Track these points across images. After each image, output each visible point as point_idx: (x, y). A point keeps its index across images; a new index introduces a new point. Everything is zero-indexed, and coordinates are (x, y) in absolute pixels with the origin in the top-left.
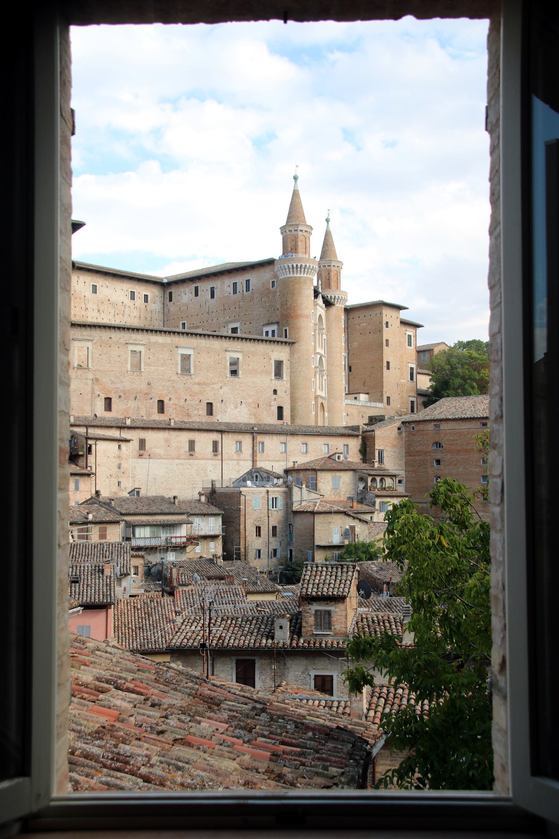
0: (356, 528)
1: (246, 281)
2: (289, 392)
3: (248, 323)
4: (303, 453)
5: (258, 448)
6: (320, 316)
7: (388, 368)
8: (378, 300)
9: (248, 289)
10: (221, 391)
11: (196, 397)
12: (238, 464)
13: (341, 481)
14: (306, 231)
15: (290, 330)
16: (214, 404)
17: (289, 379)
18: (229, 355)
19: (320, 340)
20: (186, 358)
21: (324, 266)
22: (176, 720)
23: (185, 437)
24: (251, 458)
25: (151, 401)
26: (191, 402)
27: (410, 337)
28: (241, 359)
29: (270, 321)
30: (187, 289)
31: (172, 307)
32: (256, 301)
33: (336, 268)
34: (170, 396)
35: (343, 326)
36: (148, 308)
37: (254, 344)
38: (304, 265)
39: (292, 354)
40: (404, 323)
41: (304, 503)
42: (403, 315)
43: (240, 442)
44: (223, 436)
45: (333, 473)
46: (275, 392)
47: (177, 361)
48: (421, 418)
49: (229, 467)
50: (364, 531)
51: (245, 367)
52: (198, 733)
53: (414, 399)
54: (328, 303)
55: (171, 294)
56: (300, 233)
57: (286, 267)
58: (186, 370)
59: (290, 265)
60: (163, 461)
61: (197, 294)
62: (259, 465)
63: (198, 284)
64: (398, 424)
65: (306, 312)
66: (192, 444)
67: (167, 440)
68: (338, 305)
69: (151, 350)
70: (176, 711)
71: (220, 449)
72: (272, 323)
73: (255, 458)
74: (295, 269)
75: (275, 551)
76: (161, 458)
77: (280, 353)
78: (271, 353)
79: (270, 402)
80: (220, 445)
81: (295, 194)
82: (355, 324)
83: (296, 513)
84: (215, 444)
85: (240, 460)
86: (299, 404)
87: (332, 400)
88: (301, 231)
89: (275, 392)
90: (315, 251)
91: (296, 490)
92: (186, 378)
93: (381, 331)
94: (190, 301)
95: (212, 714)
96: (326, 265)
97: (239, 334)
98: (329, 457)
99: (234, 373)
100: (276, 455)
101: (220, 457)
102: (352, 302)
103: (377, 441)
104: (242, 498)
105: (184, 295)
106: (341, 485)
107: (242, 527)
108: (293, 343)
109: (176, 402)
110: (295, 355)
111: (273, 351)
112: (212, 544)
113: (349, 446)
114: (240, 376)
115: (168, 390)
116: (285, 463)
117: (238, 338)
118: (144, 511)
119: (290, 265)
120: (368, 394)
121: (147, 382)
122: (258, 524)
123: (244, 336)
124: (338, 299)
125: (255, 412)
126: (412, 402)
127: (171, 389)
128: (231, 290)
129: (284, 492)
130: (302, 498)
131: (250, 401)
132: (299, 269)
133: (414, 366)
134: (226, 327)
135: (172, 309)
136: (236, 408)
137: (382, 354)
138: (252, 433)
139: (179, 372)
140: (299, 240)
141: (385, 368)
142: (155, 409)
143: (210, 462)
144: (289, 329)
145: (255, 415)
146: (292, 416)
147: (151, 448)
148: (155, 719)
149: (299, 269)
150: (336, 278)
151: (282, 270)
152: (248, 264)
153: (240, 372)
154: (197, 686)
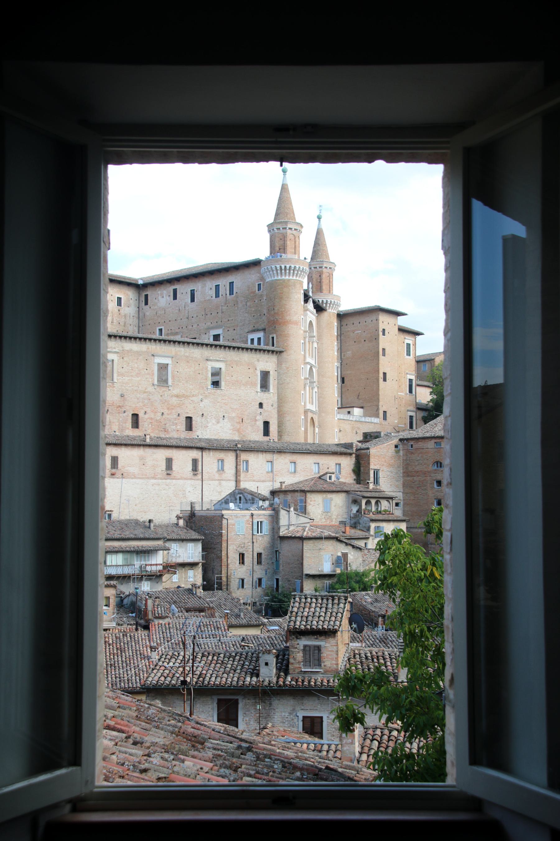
0: (349, 555)
1: (230, 283)
2: (276, 405)
3: (231, 330)
4: (291, 473)
5: (242, 467)
6: (311, 322)
7: (385, 380)
8: (374, 305)
9: (231, 293)
10: (202, 404)
11: (174, 411)
12: (220, 484)
13: (333, 503)
14: (295, 229)
15: (277, 338)
16: (193, 419)
17: (276, 391)
18: (211, 365)
19: (312, 349)
20: (163, 368)
22: (159, 759)
23: (161, 455)
24: (233, 478)
25: (125, 415)
26: (168, 417)
27: (408, 345)
28: (223, 370)
29: (256, 327)
30: (165, 292)
31: (148, 311)
32: (240, 305)
34: (146, 409)
35: (336, 334)
36: (122, 311)
37: (237, 353)
38: (293, 266)
39: (279, 364)
40: (402, 330)
41: (292, 528)
42: (402, 321)
43: (222, 461)
44: (204, 453)
45: (324, 495)
46: (261, 405)
47: (153, 371)
48: (421, 435)
49: (210, 487)
50: (357, 559)
51: (228, 378)
52: (182, 772)
54: (319, 309)
55: (146, 296)
56: (289, 231)
57: (274, 269)
58: (163, 381)
59: (278, 266)
60: (138, 481)
61: (175, 298)
62: (243, 485)
63: (177, 286)
64: (395, 441)
65: (295, 318)
66: (169, 462)
67: (142, 458)
68: (330, 310)
69: (125, 359)
70: (159, 749)
71: (200, 468)
72: (258, 330)
73: (239, 478)
74: (283, 271)
76: (135, 478)
77: (267, 363)
78: (256, 363)
79: (256, 417)
80: (200, 463)
81: (284, 189)
82: (348, 331)
83: (283, 538)
84: (195, 462)
85: (222, 480)
86: (288, 418)
87: (323, 414)
88: (290, 229)
89: (261, 405)
90: (306, 250)
91: (283, 513)
92: (164, 389)
93: (377, 339)
94: (168, 305)
95: (196, 753)
96: (318, 266)
97: (221, 342)
98: (320, 478)
99: (216, 384)
100: (263, 475)
101: (200, 477)
102: (346, 306)
103: (372, 460)
104: (224, 522)
105: (161, 298)
106: (333, 508)
107: (224, 553)
108: (281, 352)
109: (152, 416)
110: (283, 365)
111: (258, 361)
112: (191, 573)
113: (342, 465)
114: (222, 388)
115: (143, 403)
116: (271, 483)
117: (221, 346)
118: (117, 536)
119: (278, 266)
120: (362, 408)
121: (120, 393)
122: (241, 551)
124: (330, 304)
125: (238, 427)
126: (411, 417)
127: (146, 401)
128: (213, 293)
132: (288, 271)
133: (413, 377)
134: (208, 334)
135: (147, 314)
136: (218, 422)
137: (378, 364)
138: (236, 450)
139: (156, 382)
140: (288, 239)
141: (381, 380)
142: (129, 424)
143: (189, 482)
144: (277, 336)
145: (238, 430)
146: (279, 432)
147: (123, 467)
148: (137, 757)
149: (288, 271)
150: (328, 281)
151: (269, 272)
152: (232, 265)
153: (223, 384)
154: (180, 724)
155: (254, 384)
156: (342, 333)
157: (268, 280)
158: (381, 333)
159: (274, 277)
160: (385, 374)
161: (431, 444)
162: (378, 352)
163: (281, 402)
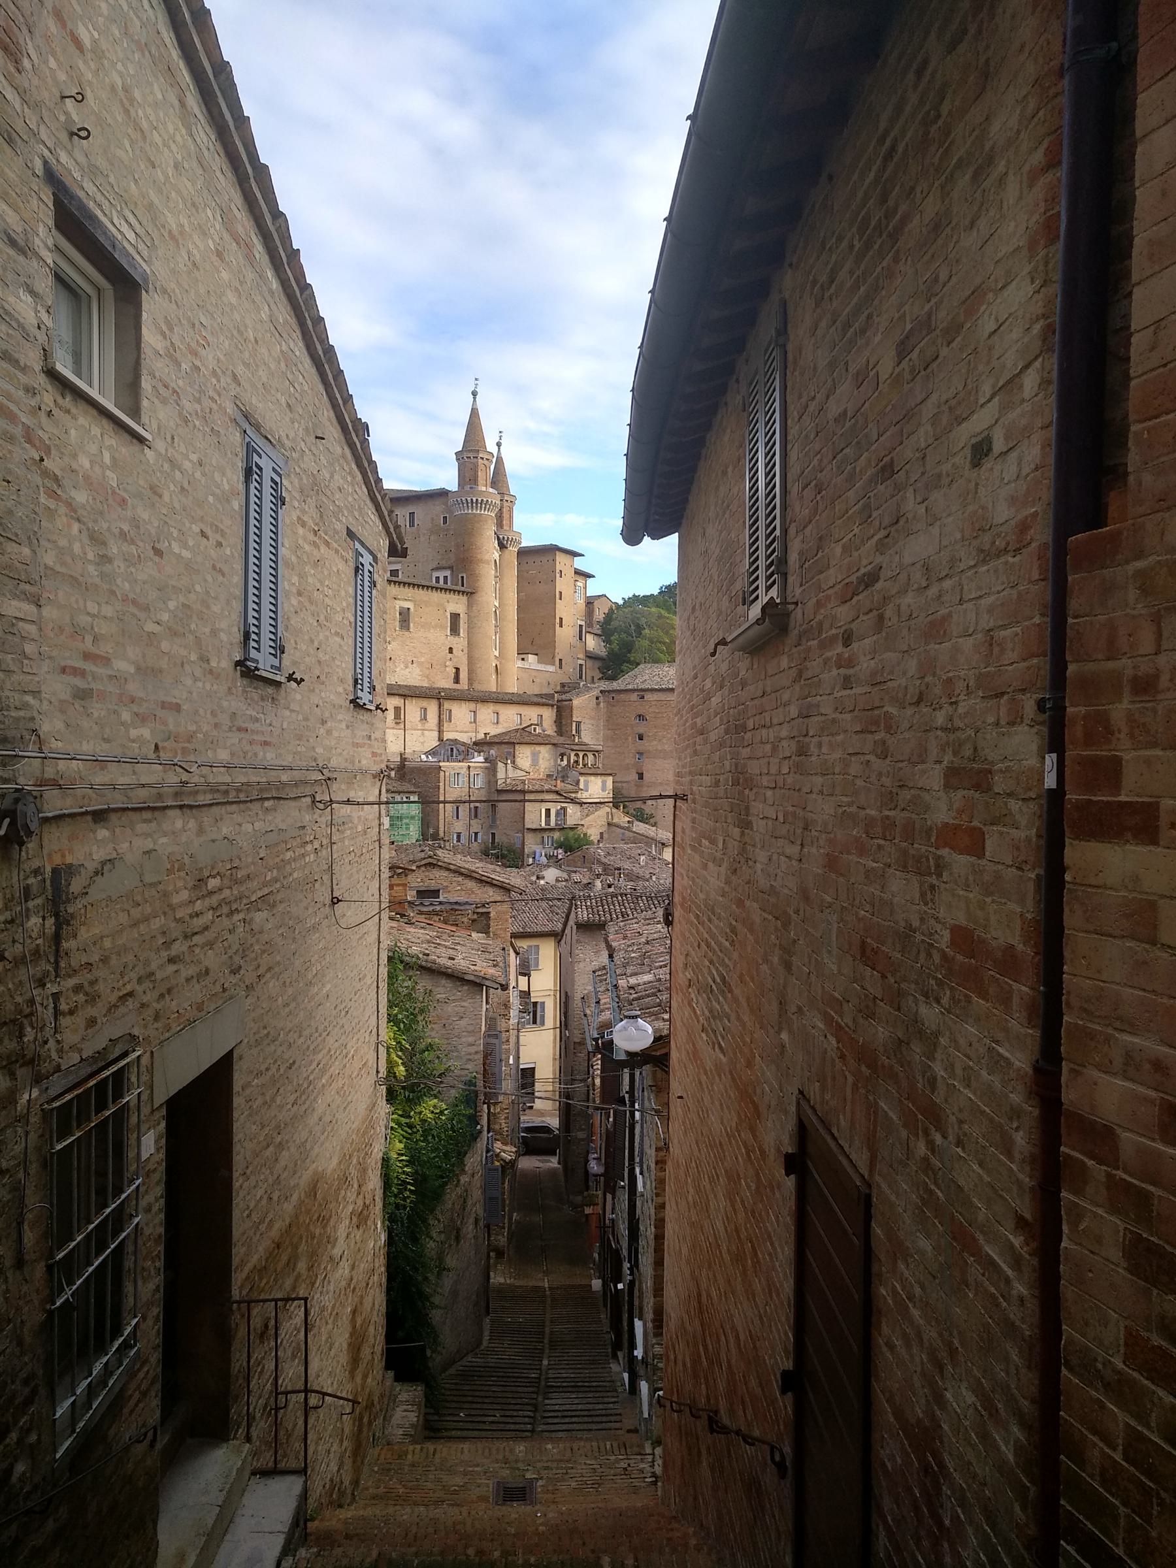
2: (466, 651)
5: (445, 717)
7: (561, 626)
18: (399, 604)
19: (498, 589)
24: (436, 728)
28: (412, 610)
32: (422, 539)
33: (509, 504)
39: (470, 605)
40: (578, 573)
41: (508, 781)
42: (578, 563)
45: (533, 747)
48: (623, 688)
53: (583, 662)
62: (447, 736)
64: (596, 692)
65: (486, 557)
72: (444, 568)
75: (476, 834)
77: (457, 604)
81: (474, 414)
83: (499, 792)
91: (500, 765)
93: (553, 581)
97: (400, 577)
100: (466, 724)
102: (526, 543)
103: (574, 712)
104: (442, 774)
106: (541, 761)
117: (400, 583)
123: (405, 580)
129: (486, 768)
130: (505, 774)
131: (423, 660)
133: (583, 623)
145: (427, 677)
155: (443, 627)
160: (561, 619)
161: (634, 697)
163: (471, 645)
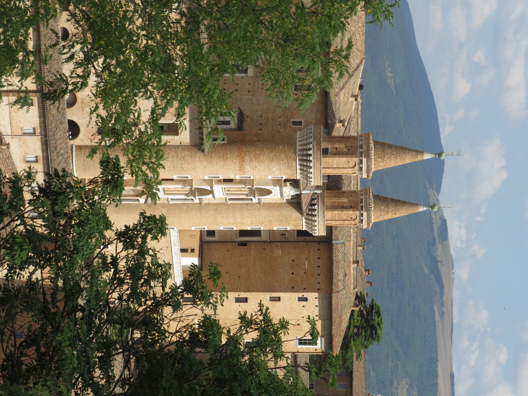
3: (249, 88)
6: (269, 192)
14: (361, 169)
21: (362, 200)
29: (246, 119)
35: (275, 229)
38: (311, 164)
65: (247, 167)
73: (11, 94)
82: (310, 252)
93: (293, 289)
110: (187, 152)
116: (10, 133)
119: (311, 146)
140: (349, 159)
144: (224, 144)
150: (345, 218)
151: (307, 135)
156: (309, 244)
157: (298, 133)
158: (300, 295)
159: (299, 141)
162: (274, 291)
